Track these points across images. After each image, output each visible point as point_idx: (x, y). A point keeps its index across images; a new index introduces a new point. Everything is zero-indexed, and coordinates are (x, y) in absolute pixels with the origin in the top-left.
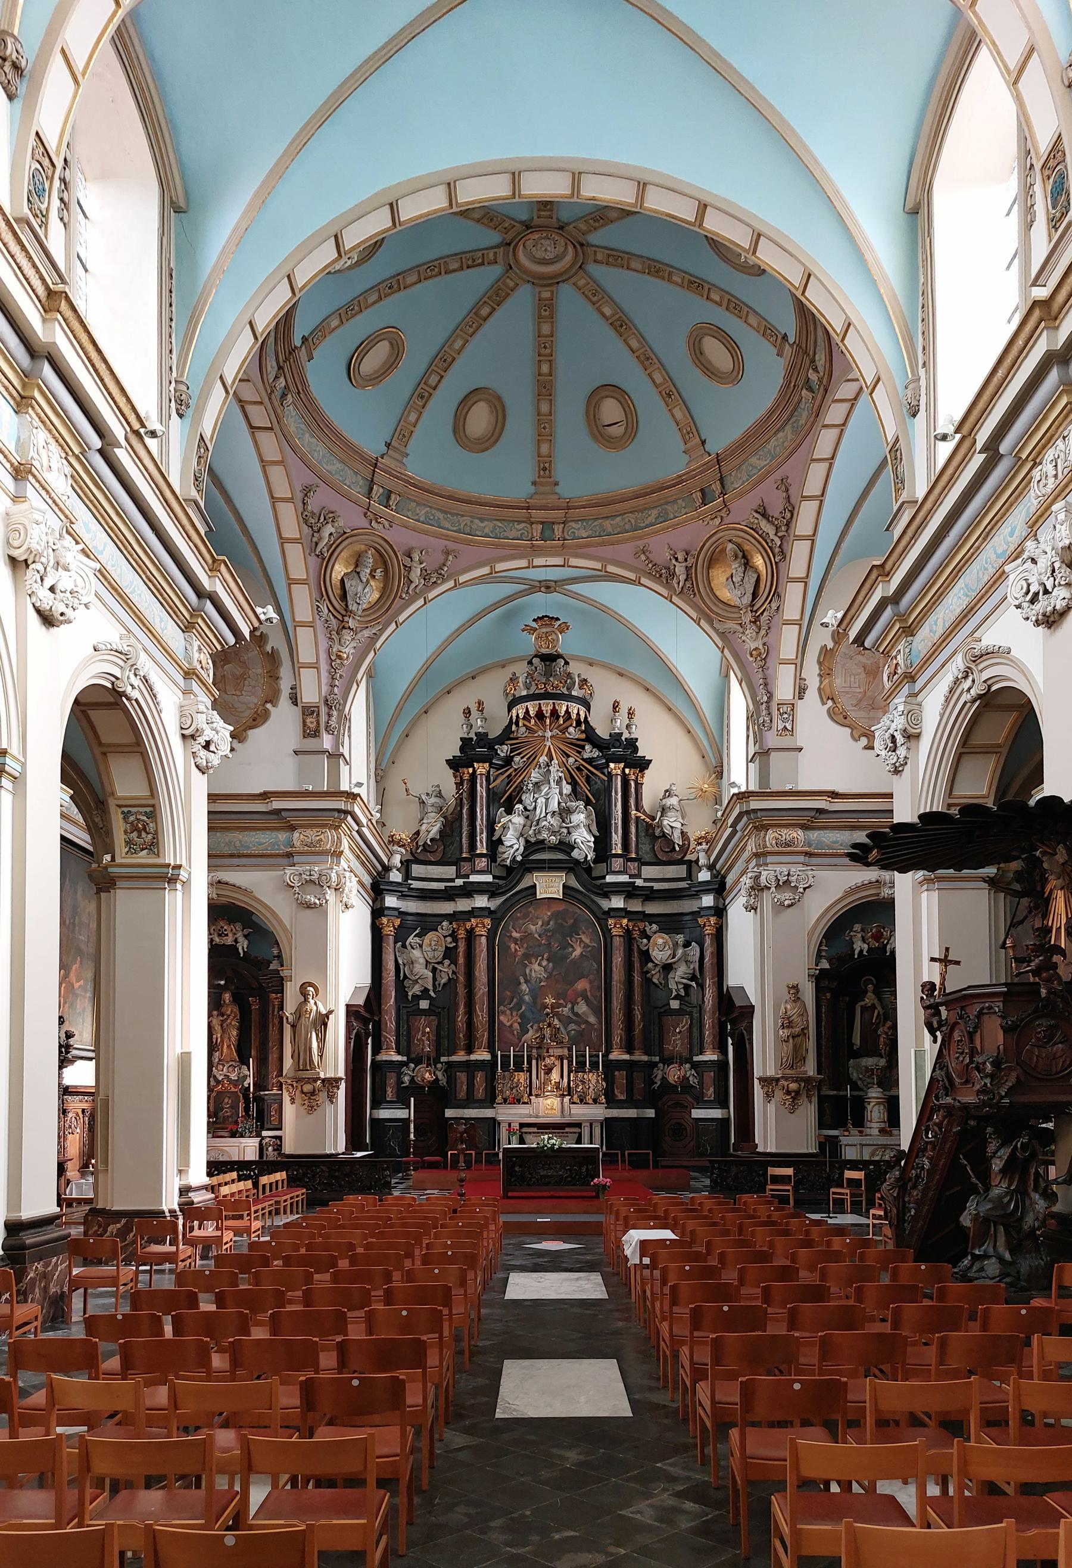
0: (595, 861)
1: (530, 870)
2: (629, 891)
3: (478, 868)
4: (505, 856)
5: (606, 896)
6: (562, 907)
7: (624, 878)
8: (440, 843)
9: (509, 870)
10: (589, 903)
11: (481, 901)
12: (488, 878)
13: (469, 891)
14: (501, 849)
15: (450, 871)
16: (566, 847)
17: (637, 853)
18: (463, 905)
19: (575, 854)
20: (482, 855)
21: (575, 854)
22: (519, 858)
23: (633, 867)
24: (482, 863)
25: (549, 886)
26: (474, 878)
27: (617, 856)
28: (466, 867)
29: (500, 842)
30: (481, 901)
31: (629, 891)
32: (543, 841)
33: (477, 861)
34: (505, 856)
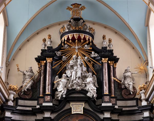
0: (97, 98)
1: (69, 102)
2: (112, 110)
3: (46, 100)
4: (58, 96)
5: (102, 113)
6: (83, 117)
7: (110, 104)
8: (31, 91)
9: (60, 101)
10: (95, 116)
11: (47, 115)
12: (51, 104)
13: (43, 110)
14: (57, 93)
15: (34, 103)
16: (85, 92)
17: (115, 95)
18: (39, 117)
19: (89, 94)
20: (48, 95)
21: (89, 94)
22: (64, 96)
23: (113, 100)
24: (48, 98)
25: (78, 108)
26: (44, 104)
27: (106, 95)
28: (41, 100)
29: (56, 90)
30: (47, 115)
31: (112, 110)
32: (75, 89)
33: (46, 97)
34: (58, 96)
